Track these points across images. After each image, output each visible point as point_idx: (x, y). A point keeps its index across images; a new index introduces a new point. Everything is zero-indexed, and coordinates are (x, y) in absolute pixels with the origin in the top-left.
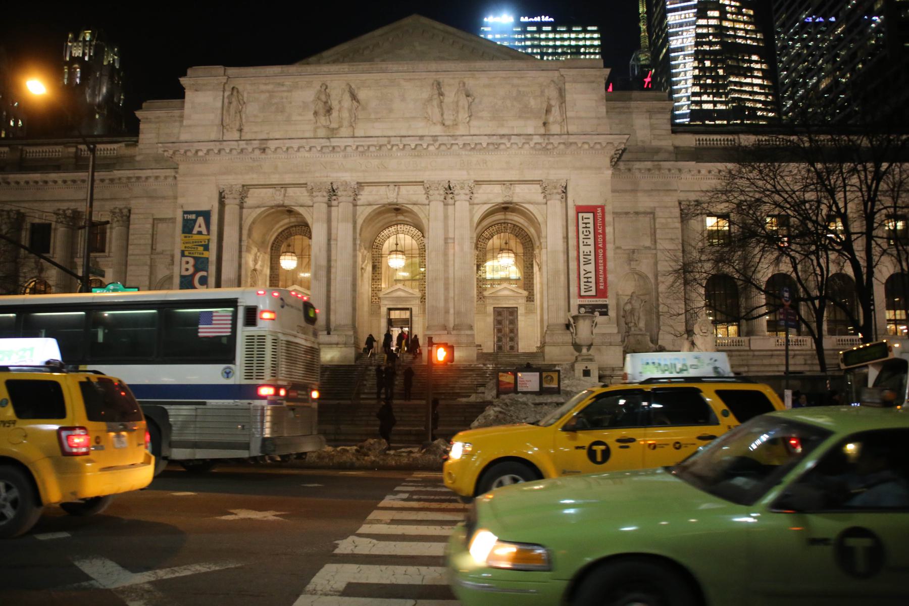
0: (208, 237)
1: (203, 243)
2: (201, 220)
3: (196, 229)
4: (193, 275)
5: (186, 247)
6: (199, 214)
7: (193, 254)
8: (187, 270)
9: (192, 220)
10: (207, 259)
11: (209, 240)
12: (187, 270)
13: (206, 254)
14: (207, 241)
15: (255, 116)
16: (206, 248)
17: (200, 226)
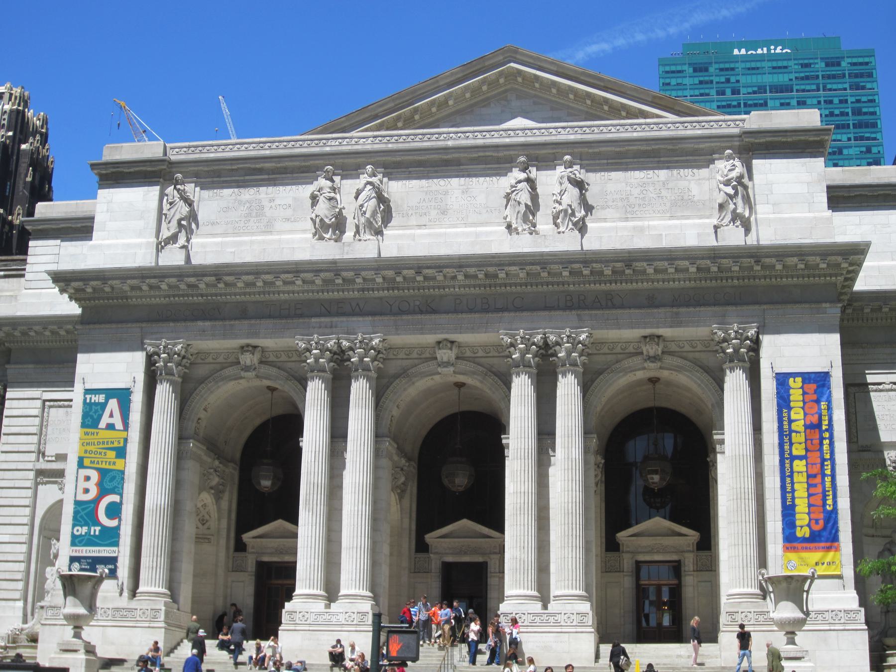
0: (124, 434)
1: (116, 445)
2: (113, 404)
3: (105, 420)
4: (97, 501)
5: (86, 452)
6: (110, 393)
7: (98, 463)
8: (86, 491)
9: (96, 404)
10: (123, 472)
11: (126, 440)
12: (86, 491)
13: (119, 464)
14: (122, 441)
15: (213, 224)
16: (121, 453)
17: (111, 416)
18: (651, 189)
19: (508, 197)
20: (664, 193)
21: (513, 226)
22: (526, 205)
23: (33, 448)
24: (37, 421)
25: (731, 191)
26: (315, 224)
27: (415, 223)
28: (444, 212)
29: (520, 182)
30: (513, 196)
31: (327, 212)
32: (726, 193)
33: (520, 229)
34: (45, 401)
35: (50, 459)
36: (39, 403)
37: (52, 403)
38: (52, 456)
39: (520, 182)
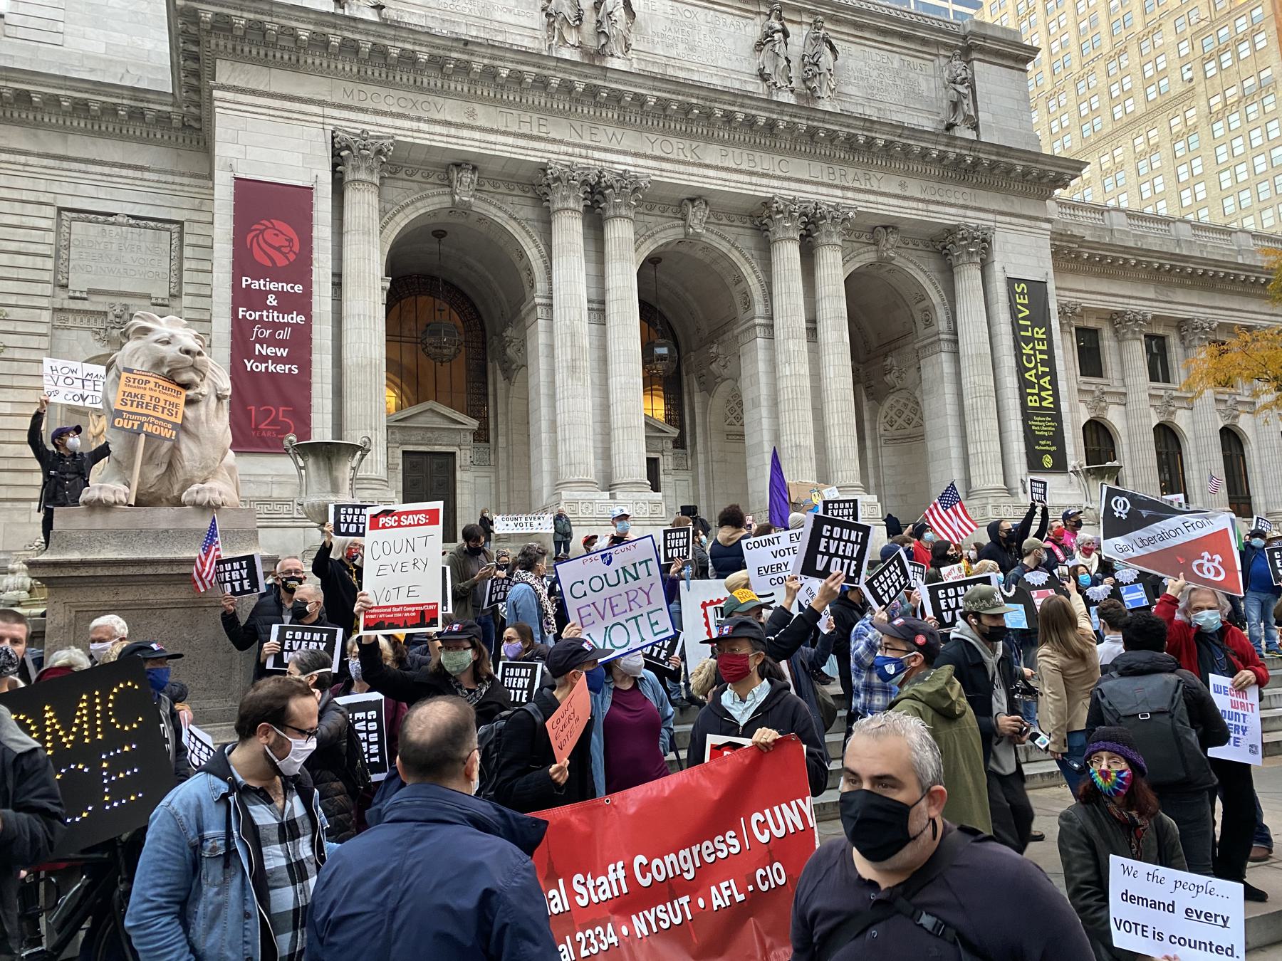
18: (887, 74)
19: (759, 47)
20: (898, 82)
21: (772, 81)
22: (786, 58)
23: (48, 276)
24: (50, 238)
25: (961, 88)
26: (550, 25)
27: (662, 53)
28: (693, 49)
29: (778, 31)
30: (769, 46)
31: (569, 11)
32: (959, 92)
33: (778, 85)
34: (60, 210)
35: (78, 294)
36: (51, 212)
37: (74, 215)
38: (81, 292)
39: (778, 31)
